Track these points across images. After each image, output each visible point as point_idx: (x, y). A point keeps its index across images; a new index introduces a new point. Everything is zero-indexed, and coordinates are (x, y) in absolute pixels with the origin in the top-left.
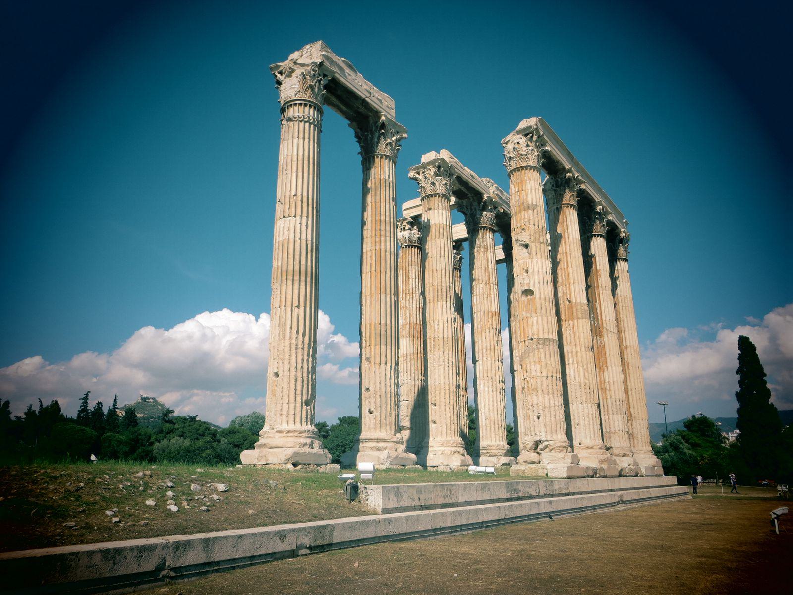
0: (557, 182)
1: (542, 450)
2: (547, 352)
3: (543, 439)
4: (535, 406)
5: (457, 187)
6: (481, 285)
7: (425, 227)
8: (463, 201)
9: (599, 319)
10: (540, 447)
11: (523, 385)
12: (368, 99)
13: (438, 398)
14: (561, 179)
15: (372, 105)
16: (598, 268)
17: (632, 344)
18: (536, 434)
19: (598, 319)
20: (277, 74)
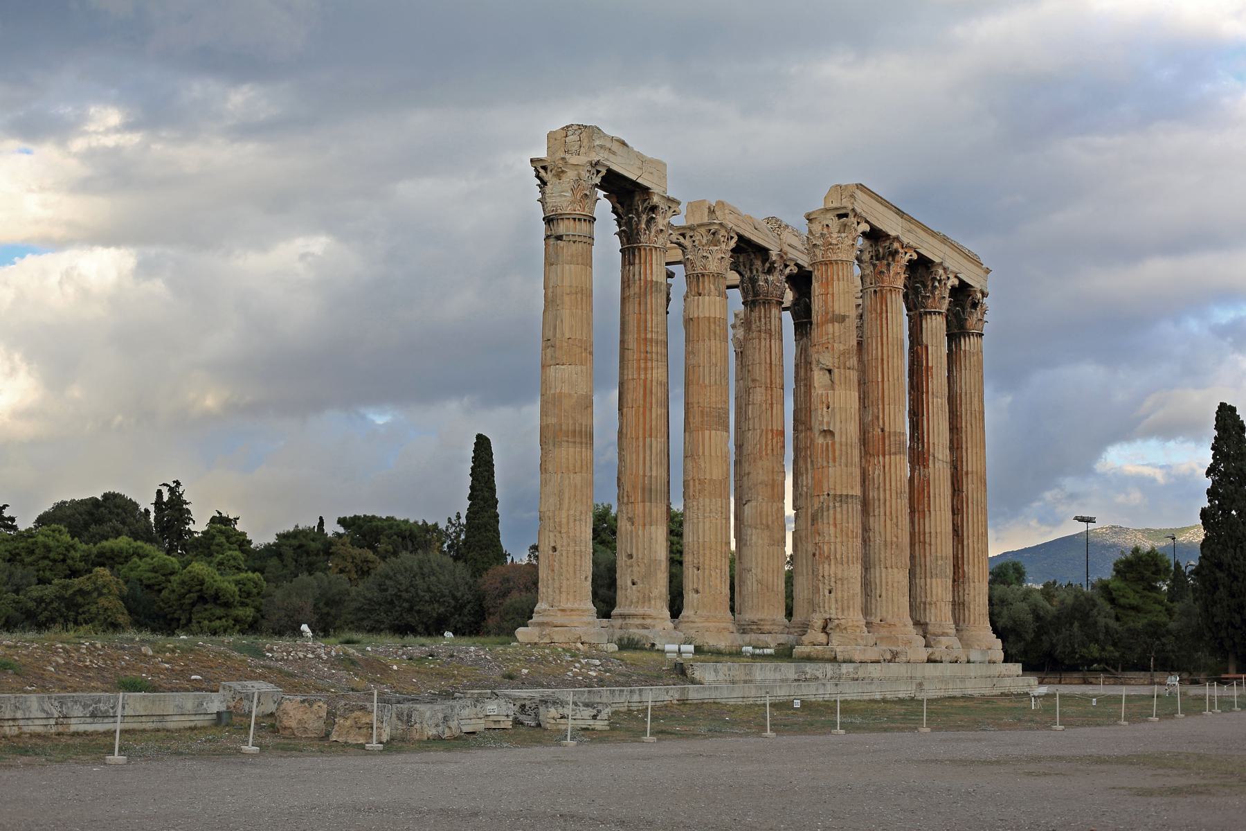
1: (831, 629)
2: (844, 512)
3: (833, 616)
4: (827, 578)
6: (758, 389)
7: (692, 319)
8: (739, 255)
9: (925, 441)
10: (830, 626)
11: (814, 551)
13: (701, 559)
16: (930, 365)
17: (975, 470)
18: (825, 612)
19: (923, 441)
20: (541, 170)
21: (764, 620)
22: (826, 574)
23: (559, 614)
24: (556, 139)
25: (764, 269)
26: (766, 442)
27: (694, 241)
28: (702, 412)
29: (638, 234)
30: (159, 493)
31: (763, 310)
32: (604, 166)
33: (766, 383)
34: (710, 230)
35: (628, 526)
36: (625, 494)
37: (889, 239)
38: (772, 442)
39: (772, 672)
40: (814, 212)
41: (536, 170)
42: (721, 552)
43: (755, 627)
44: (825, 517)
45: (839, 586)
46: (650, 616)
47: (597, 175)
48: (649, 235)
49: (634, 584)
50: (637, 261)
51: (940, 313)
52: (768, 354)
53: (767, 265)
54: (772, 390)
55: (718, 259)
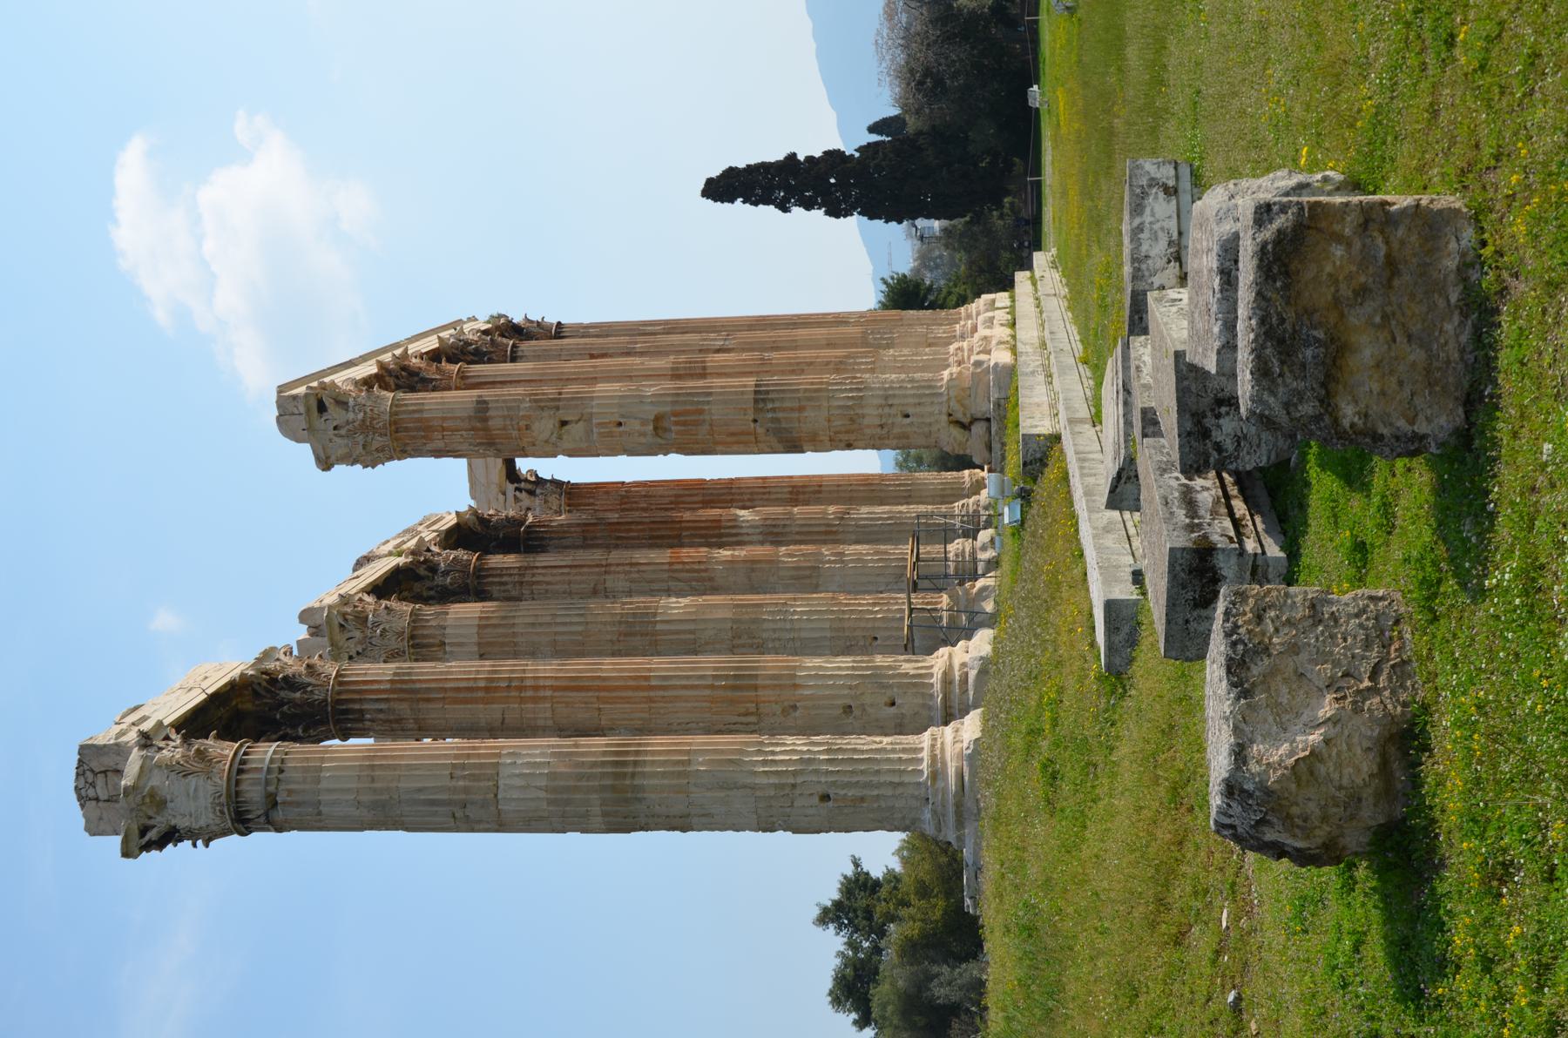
3: (944, 410)
10: (959, 416)
12: (210, 691)
15: (221, 688)
20: (147, 838)
22: (877, 422)
23: (940, 784)
24: (101, 819)
26: (688, 571)
27: (358, 653)
28: (626, 635)
29: (311, 705)
31: (490, 579)
33: (599, 574)
34: (342, 626)
36: (743, 719)
37: (382, 376)
38: (687, 563)
41: (147, 847)
45: (895, 401)
48: (314, 686)
49: (893, 704)
50: (357, 706)
51: (514, 346)
52: (555, 571)
53: (422, 571)
54: (610, 565)
55: (388, 614)
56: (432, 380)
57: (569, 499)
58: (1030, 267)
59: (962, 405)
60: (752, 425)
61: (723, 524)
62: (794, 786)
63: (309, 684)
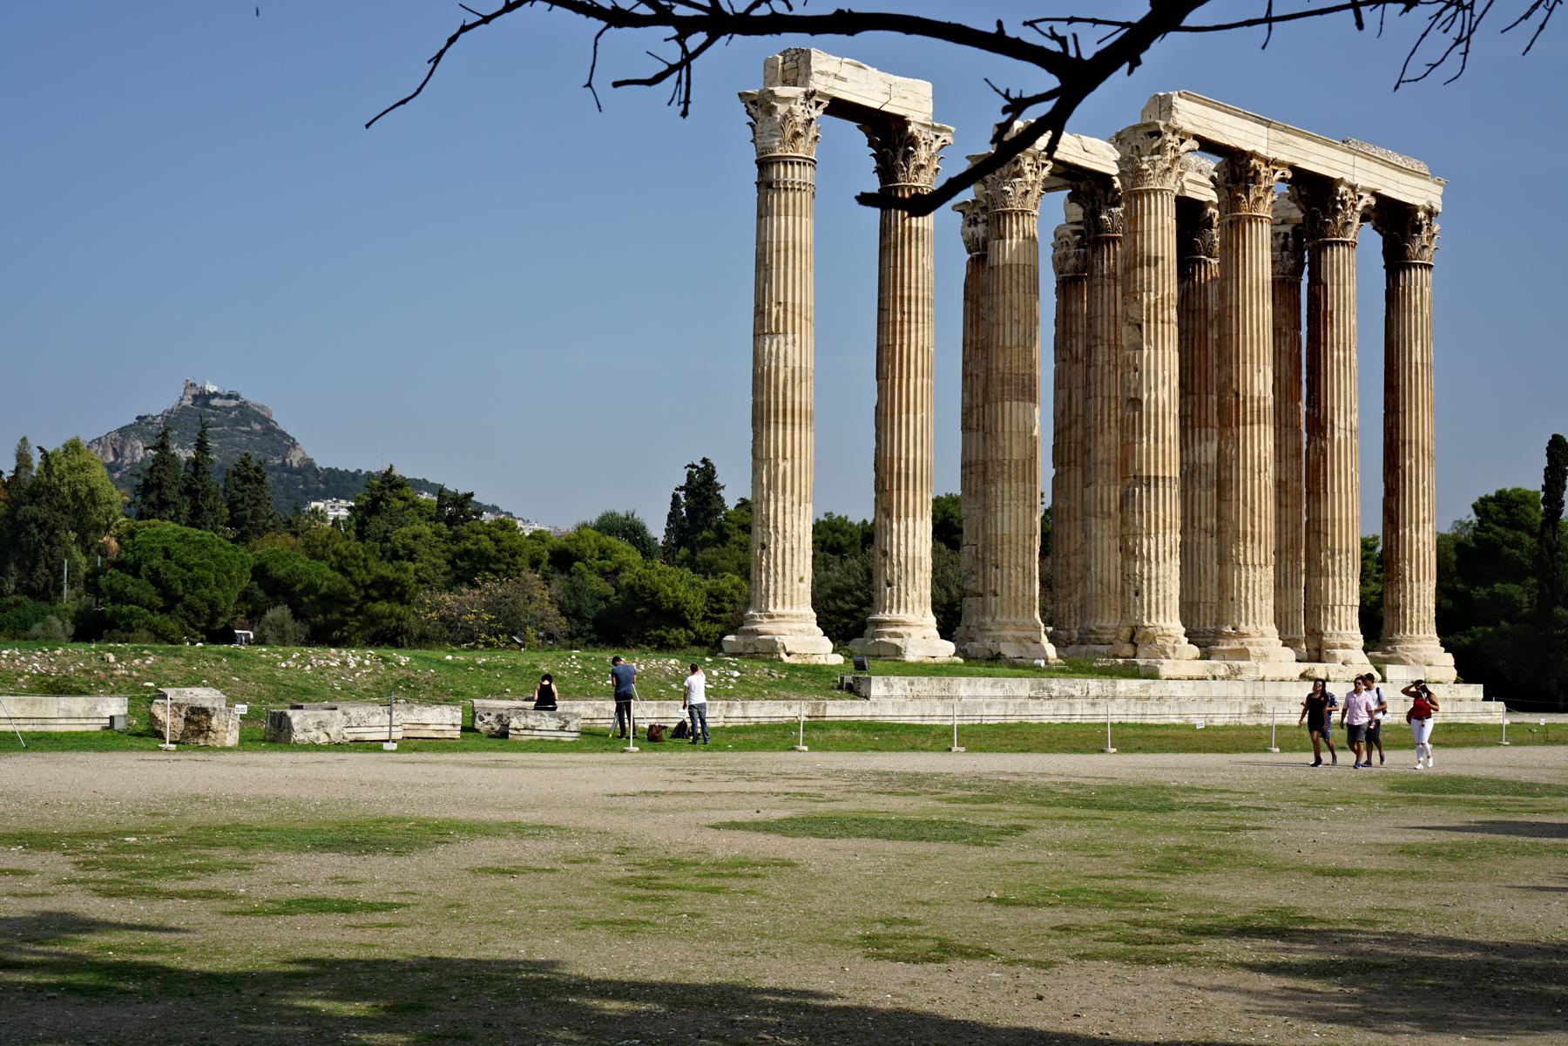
0: (1233, 173)
3: (1139, 624)
5: (1061, 169)
9: (1322, 404)
14: (1240, 167)
20: (750, 106)
21: (1105, 628)
23: (766, 620)
25: (1107, 200)
26: (1109, 412)
28: (1003, 379)
30: (690, 475)
32: (823, 95)
33: (1109, 340)
35: (883, 518)
39: (989, 689)
40: (1122, 131)
42: (1024, 547)
43: (1093, 637)
44: (1130, 504)
46: (904, 624)
47: (817, 107)
52: (1112, 305)
53: (1110, 195)
56: (1247, 195)
57: (1290, 282)
58: (1487, 698)
59: (1144, 637)
60: (1132, 475)
61: (1203, 430)
62: (768, 527)
63: (908, 168)
